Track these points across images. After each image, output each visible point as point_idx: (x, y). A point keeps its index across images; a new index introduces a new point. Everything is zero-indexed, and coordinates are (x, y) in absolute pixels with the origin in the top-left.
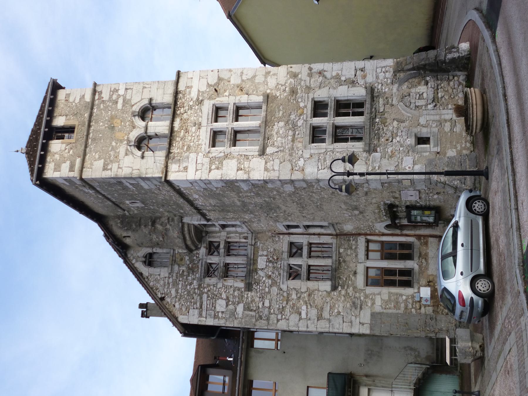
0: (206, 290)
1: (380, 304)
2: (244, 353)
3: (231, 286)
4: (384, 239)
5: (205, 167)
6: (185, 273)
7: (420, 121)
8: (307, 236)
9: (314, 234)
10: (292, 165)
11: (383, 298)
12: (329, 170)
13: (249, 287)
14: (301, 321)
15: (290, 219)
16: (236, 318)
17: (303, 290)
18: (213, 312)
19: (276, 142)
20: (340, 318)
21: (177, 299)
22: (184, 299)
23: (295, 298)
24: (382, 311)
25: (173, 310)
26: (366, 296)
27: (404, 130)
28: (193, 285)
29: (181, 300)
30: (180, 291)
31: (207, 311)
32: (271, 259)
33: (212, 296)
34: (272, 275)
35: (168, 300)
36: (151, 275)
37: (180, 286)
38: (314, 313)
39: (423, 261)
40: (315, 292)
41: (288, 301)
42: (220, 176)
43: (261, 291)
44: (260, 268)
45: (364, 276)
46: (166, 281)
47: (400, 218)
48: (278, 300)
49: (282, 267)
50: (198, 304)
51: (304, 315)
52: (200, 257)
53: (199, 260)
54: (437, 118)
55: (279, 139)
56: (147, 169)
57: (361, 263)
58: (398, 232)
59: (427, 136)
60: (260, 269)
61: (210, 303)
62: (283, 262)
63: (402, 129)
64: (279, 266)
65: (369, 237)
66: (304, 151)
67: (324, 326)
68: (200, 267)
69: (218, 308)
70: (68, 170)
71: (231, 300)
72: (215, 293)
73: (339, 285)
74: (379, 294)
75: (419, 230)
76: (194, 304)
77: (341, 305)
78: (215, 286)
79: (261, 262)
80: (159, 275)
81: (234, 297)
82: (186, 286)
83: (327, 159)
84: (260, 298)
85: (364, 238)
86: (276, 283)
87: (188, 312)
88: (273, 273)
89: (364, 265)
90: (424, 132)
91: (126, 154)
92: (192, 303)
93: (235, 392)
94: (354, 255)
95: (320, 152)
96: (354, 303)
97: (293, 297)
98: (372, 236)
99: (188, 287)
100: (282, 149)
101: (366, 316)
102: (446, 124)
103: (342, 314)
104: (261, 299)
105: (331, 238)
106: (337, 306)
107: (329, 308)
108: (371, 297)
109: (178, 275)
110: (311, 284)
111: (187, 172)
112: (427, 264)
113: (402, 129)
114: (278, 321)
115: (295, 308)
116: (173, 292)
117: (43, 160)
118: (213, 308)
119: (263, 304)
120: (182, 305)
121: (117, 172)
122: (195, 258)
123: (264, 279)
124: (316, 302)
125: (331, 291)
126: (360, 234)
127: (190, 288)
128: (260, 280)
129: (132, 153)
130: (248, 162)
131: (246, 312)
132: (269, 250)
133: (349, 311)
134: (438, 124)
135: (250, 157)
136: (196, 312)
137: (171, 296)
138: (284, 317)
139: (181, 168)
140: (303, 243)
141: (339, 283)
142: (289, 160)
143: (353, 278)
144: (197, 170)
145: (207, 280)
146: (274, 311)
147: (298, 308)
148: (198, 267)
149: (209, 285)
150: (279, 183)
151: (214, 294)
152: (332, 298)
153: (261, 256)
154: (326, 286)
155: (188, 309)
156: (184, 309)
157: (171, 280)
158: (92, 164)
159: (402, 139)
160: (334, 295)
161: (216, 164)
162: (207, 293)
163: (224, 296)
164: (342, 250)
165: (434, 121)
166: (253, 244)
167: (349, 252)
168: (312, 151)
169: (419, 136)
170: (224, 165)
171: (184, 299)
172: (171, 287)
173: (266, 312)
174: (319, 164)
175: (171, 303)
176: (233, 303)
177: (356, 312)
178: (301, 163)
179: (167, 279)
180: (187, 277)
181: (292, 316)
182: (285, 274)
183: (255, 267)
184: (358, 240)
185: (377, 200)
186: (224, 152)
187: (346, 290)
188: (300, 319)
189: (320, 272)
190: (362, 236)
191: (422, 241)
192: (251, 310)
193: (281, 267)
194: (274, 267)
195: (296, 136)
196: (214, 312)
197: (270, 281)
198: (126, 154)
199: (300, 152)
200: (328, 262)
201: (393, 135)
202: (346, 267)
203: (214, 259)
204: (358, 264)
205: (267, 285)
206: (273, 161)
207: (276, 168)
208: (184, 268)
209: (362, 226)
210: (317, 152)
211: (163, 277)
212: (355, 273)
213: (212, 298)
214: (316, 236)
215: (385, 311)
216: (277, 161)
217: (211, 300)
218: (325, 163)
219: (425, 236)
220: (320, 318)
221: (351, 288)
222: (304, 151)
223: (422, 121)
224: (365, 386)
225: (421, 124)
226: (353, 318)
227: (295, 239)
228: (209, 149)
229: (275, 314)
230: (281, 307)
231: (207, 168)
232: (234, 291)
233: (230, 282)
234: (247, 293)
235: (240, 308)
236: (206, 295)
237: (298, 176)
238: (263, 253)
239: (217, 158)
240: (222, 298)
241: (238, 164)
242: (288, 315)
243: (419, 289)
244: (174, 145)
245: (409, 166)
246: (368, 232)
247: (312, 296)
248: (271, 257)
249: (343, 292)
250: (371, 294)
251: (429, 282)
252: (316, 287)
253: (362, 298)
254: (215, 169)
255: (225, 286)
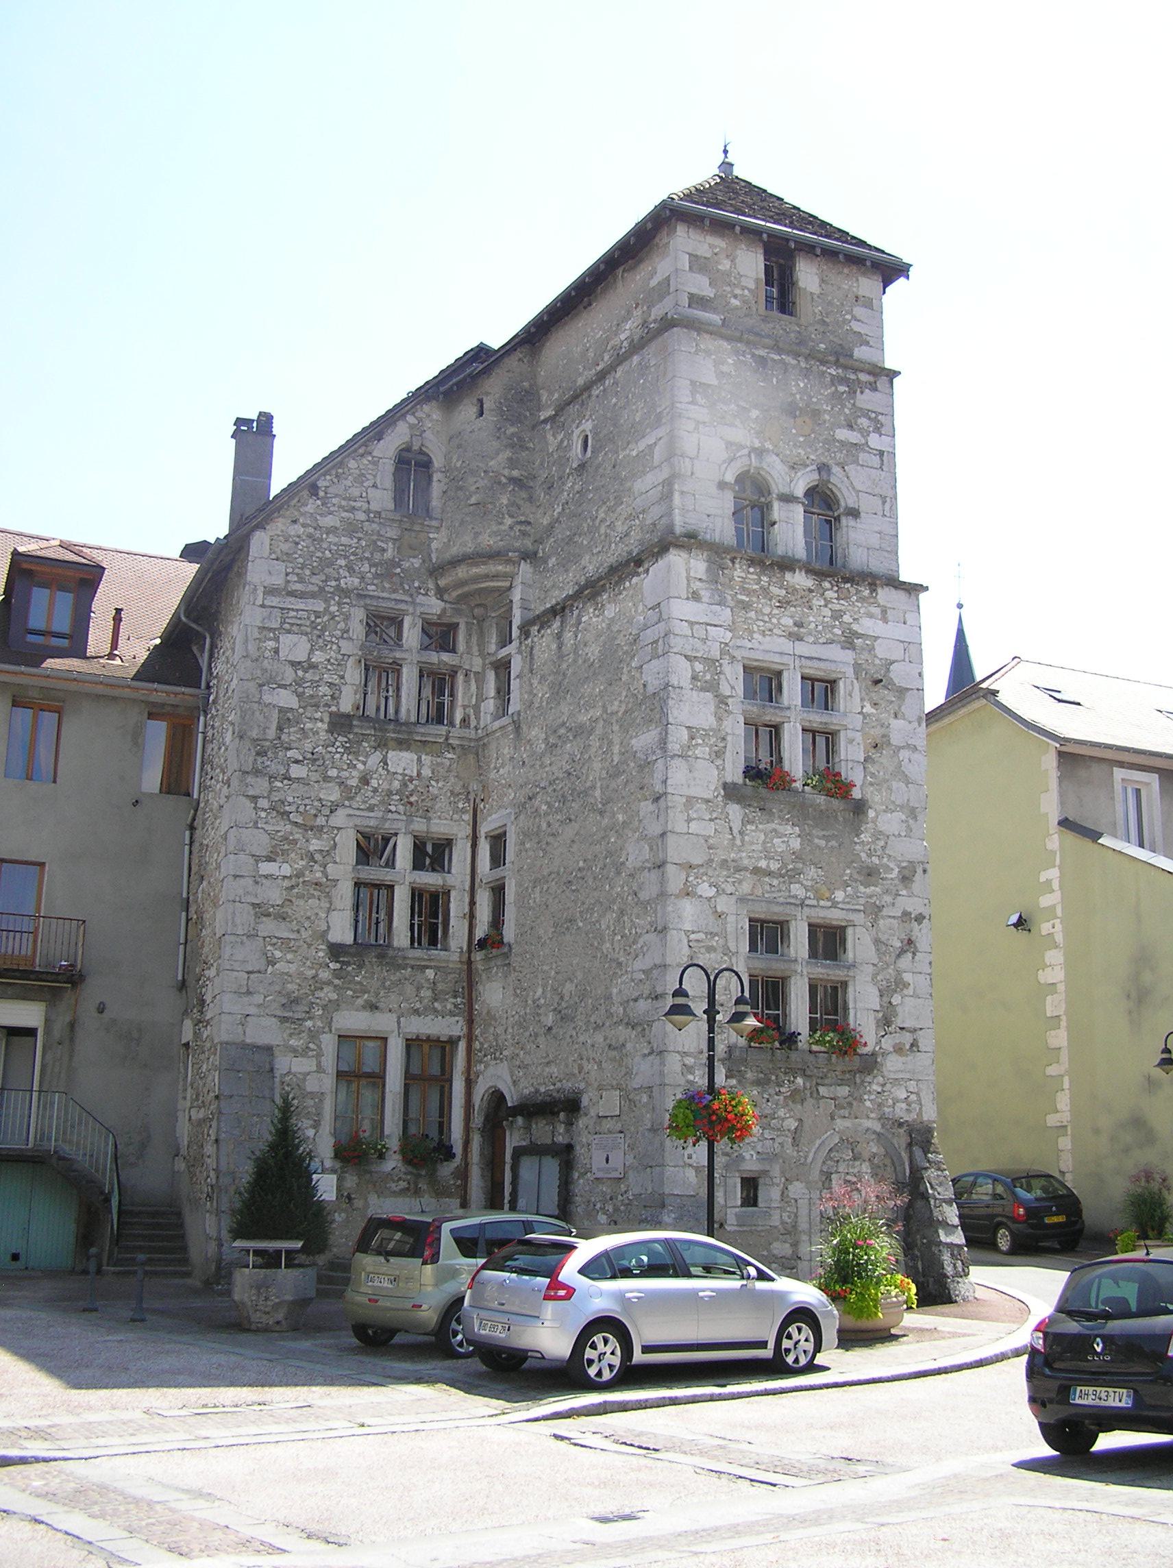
0: (334, 609)
1: (293, 1070)
2: (134, 695)
3: (342, 677)
4: (458, 1086)
5: (698, 644)
6: (377, 556)
7: (796, 1183)
8: (467, 886)
9: (472, 903)
10: (699, 866)
11: (308, 1077)
12: (685, 961)
13: (340, 723)
14: (252, 861)
15: (528, 846)
16: (261, 685)
17: (330, 868)
18: (277, 626)
19: (754, 828)
20: (260, 965)
21: (311, 530)
22: (312, 549)
23: (312, 848)
24: (277, 1074)
25: (284, 517)
26: (314, 1035)
27: (776, 1145)
28: (348, 574)
29: (309, 541)
30: (332, 538)
31: (282, 609)
32: (411, 787)
33: (319, 624)
34: (370, 788)
35: (311, 506)
36: (375, 463)
37: (344, 540)
38: (274, 895)
39: (403, 1184)
40: (327, 900)
41: (306, 828)
42: (676, 683)
43: (328, 756)
44: (389, 755)
45: (365, 1031)
46: (358, 504)
47: (528, 1128)
48: (307, 801)
49: (390, 816)
50: (298, 587)
51: (266, 868)
52: (420, 599)
53: (411, 596)
54: (803, 1225)
55: (762, 837)
56: (694, 495)
57: (399, 1023)
58: (478, 1120)
59: (760, 1199)
60: (385, 757)
61: (300, 619)
62: (404, 818)
63: (779, 1140)
64: (393, 808)
65: (462, 1046)
66: (733, 898)
67: (238, 921)
68: (394, 596)
69: (286, 640)
70: (694, 291)
71: (308, 676)
72: (327, 633)
73: (343, 963)
74: (320, 1069)
75: (483, 1176)
76: (298, 574)
77: (292, 968)
78: (345, 635)
79: (402, 761)
80: (375, 486)
81: (316, 684)
82: (346, 557)
83: (713, 955)
84: (313, 754)
85: (461, 1034)
86: (350, 799)
87: (277, 560)
88: (375, 790)
89: (393, 1032)
90: (769, 1194)
91: (729, 444)
92: (300, 571)
93: (10, 663)
94: (418, 1005)
95: (728, 937)
96: (296, 1001)
97: (314, 841)
98: (464, 1053)
99: (342, 562)
100: (738, 842)
101: (265, 1031)
102: (788, 1245)
103: (270, 969)
104: (309, 756)
105: (461, 948)
106: (289, 956)
107: (286, 935)
108: (311, 1045)
109: (375, 537)
110: (345, 890)
111: (688, 599)
112: (395, 1192)
113: (779, 1140)
114: (254, 799)
115: (286, 847)
116: (328, 521)
117: (721, 227)
118: (287, 626)
119: (297, 762)
120: (297, 544)
121: (689, 418)
122: (416, 584)
123: (360, 766)
124: (302, 902)
125: (328, 941)
126: (470, 1022)
127: (341, 567)
128: (356, 754)
129: (732, 460)
130: (708, 757)
131: (275, 715)
132: (433, 783)
133: (277, 988)
134: (789, 1227)
135: (719, 762)
136: (278, 581)
137: (321, 515)
138: (263, 814)
139: (698, 583)
140: (449, 872)
141: (348, 963)
142: (711, 861)
143: (360, 1002)
144: (691, 624)
145: (359, 614)
146: (278, 790)
147: (284, 852)
148: (395, 591)
149: (347, 618)
150: (655, 829)
151: (323, 630)
152: (309, 946)
153: (419, 759)
154: (342, 932)
155: (286, 557)
156: (285, 547)
157: (361, 516)
158: (708, 353)
159: (755, 1139)
160: (318, 950)
161: (704, 673)
162: (326, 610)
163: (318, 657)
164: (430, 973)
165: (796, 1216)
166: (451, 741)
167: (426, 993)
168: (731, 919)
169: (761, 1181)
170: (702, 694)
171: (312, 549)
172: (345, 514)
173: (275, 767)
174: (701, 936)
175: (302, 514)
176: (299, 682)
177: (275, 1005)
178: (705, 890)
179: (365, 506)
180: (367, 558)
181: (265, 839)
182: (372, 823)
183: (391, 744)
184: (457, 1018)
185: (593, 1073)
186: (733, 697)
187: (329, 983)
188: (257, 859)
189: (374, 915)
190: (465, 1028)
191: (452, 1182)
192: (280, 729)
193: (390, 811)
194: (390, 793)
195: (767, 879)
196: (275, 629)
197: (353, 782)
198: (729, 444)
199: (730, 889)
200: (402, 936)
201: (766, 1117)
202: (388, 983)
203: (411, 635)
204: (394, 1016)
205: (344, 774)
206: (711, 820)
207: (694, 827)
208: (389, 555)
209: (500, 1030)
210: (728, 930)
211: (370, 495)
212: (373, 1007)
213: (314, 626)
214: (467, 910)
215: (277, 1080)
216: (710, 829)
217: (308, 623)
218: (703, 950)
219: (465, 1188)
220: (261, 910)
221: (334, 996)
222: (733, 898)
223: (796, 1189)
224: (47, 1020)
225: (790, 1187)
226: (259, 999)
227: (460, 856)
228: (740, 658)
229: (270, 792)
230: (287, 808)
231: (697, 651)
232: (331, 685)
233: (353, 675)
234: (327, 719)
235: (287, 699)
236: (322, 610)
237: (675, 879)
238: (425, 767)
239: (719, 678)
240: (312, 651)
241: (703, 730)
242: (267, 827)
243: (333, 1171)
244: (751, 570)
245: (694, 1156)
246: (477, 1045)
247: (316, 893)
248: (416, 786)
249: (325, 975)
250: (319, 1047)
251: (349, 1197)
252: (338, 903)
253: (309, 1023)
254: (693, 670)
255: (342, 660)
